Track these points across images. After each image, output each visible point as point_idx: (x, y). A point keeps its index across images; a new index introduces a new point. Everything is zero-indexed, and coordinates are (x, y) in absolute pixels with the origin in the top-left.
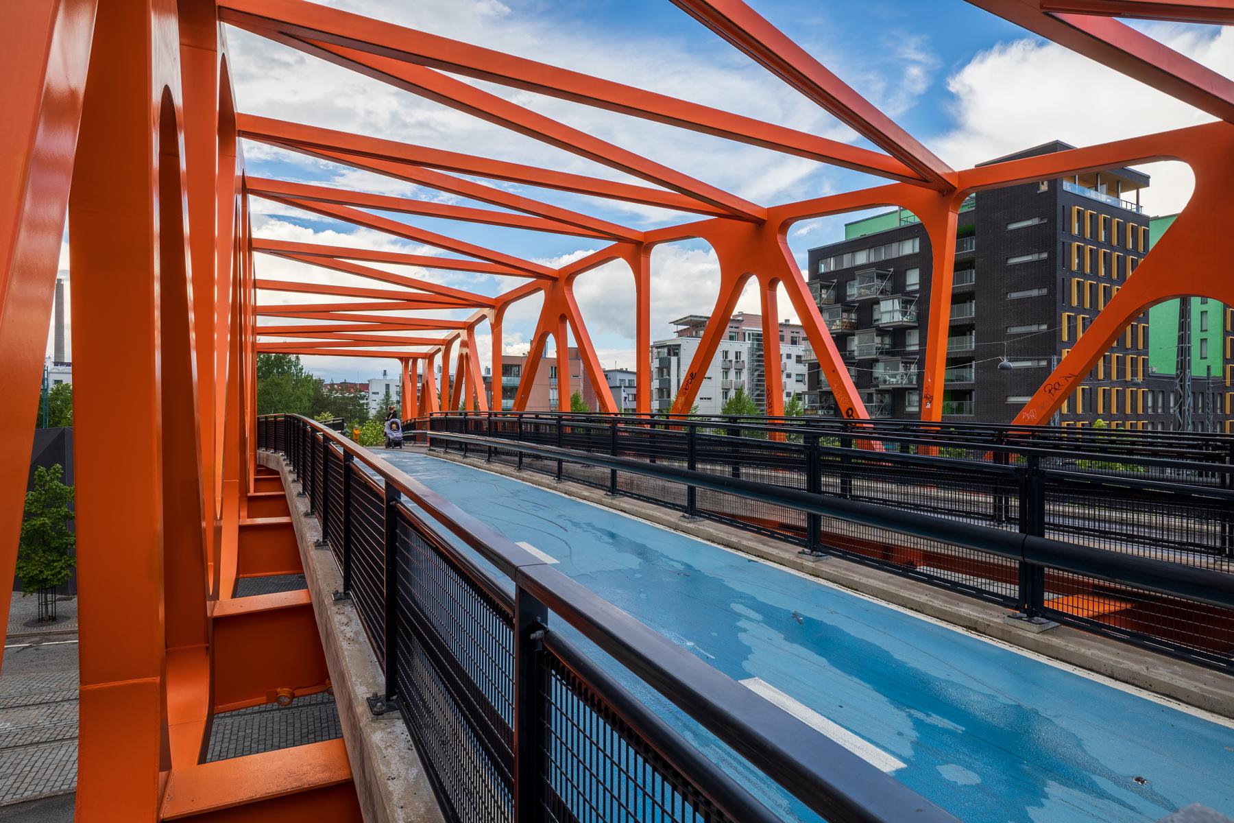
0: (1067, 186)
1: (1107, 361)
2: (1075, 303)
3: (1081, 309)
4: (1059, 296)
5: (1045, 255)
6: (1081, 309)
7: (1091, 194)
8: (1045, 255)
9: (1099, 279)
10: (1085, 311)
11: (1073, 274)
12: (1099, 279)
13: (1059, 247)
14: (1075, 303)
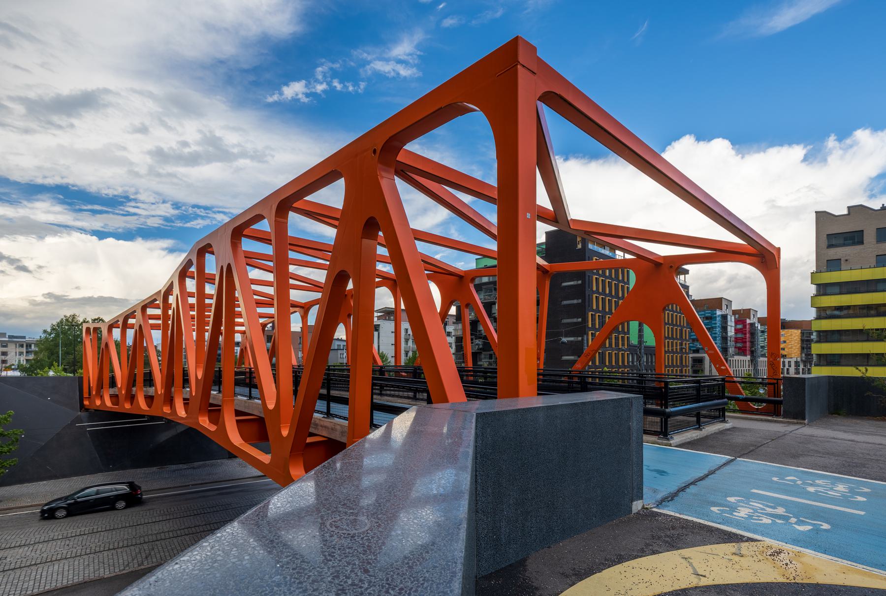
0: (590, 246)
1: (610, 339)
2: (595, 307)
3: (597, 311)
4: (587, 304)
5: (580, 282)
6: (597, 311)
7: (603, 251)
8: (580, 282)
9: (606, 295)
10: (599, 312)
11: (594, 292)
12: (606, 295)
13: (587, 278)
14: (595, 307)
